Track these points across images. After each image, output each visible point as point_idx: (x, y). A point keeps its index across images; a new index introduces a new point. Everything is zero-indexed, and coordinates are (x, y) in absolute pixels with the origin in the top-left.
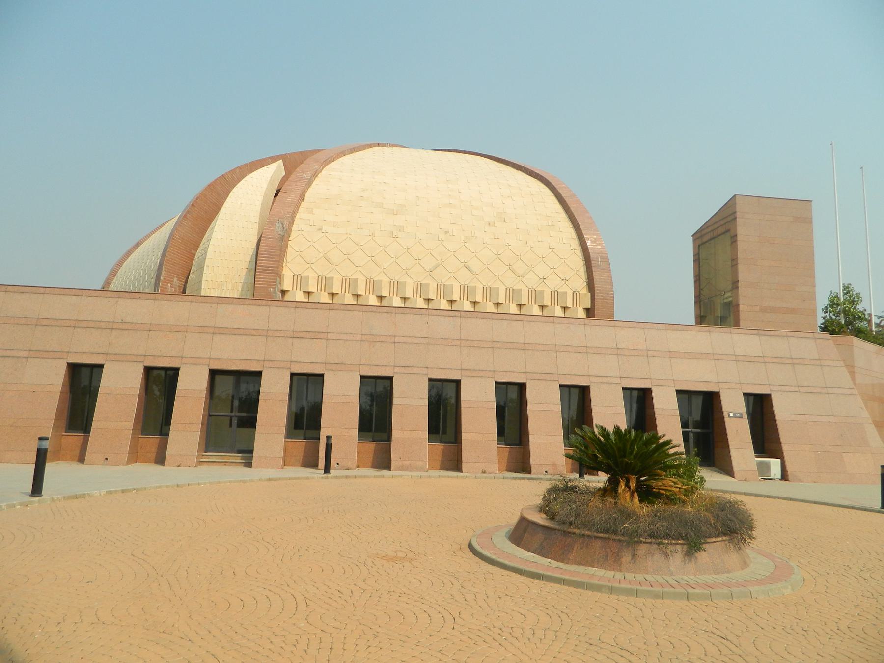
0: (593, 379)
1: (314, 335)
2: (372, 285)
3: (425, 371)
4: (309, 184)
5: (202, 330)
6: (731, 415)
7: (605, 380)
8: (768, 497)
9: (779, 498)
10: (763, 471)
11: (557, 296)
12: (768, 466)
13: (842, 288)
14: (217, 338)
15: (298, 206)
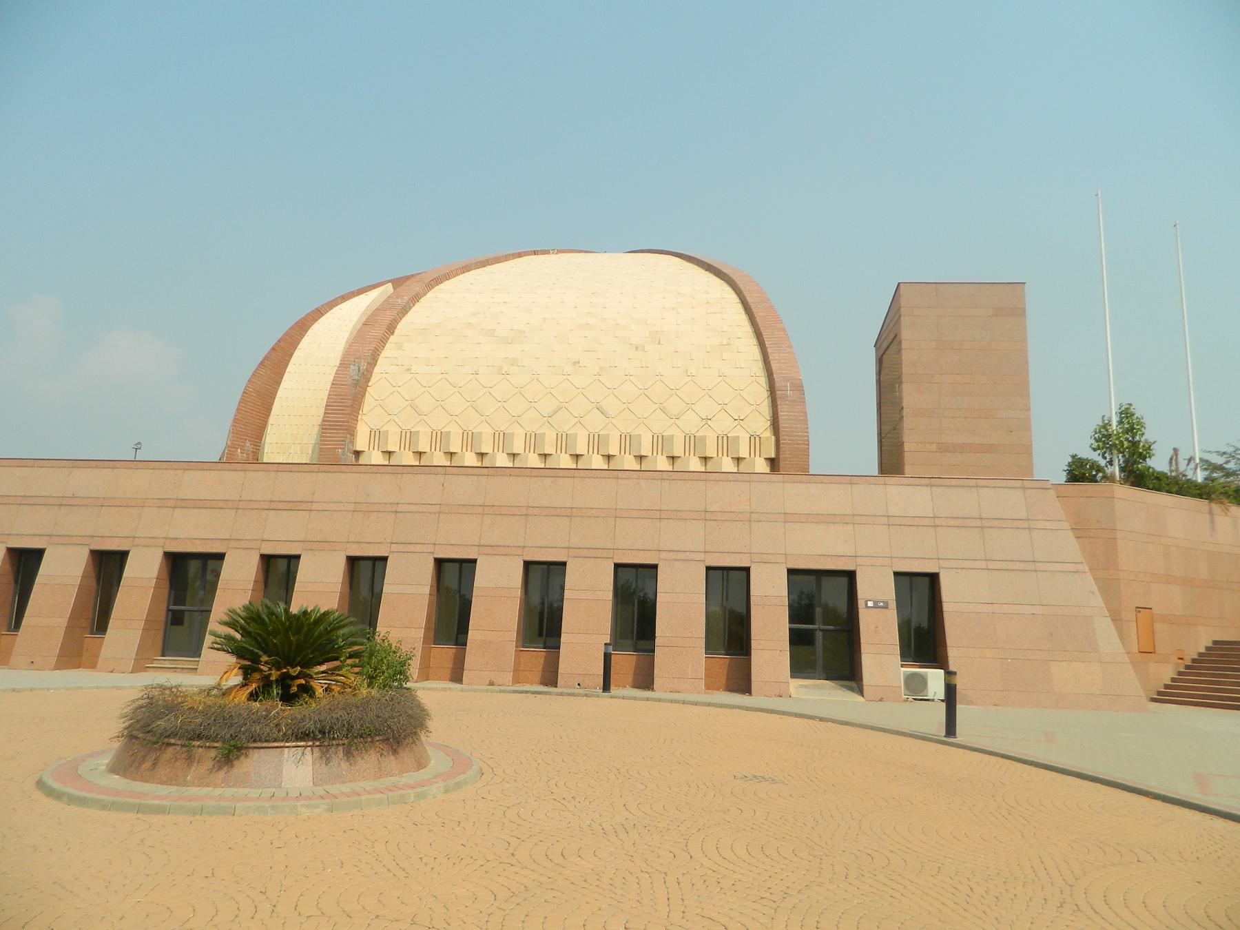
0: (664, 555)
1: (293, 506)
2: (470, 439)
3: (431, 549)
4: (404, 311)
5: (162, 503)
6: (870, 604)
7: (683, 556)
8: (822, 719)
9: (833, 721)
10: (916, 687)
11: (727, 443)
12: (923, 681)
13: (1114, 409)
14: (178, 512)
15: (383, 341)
